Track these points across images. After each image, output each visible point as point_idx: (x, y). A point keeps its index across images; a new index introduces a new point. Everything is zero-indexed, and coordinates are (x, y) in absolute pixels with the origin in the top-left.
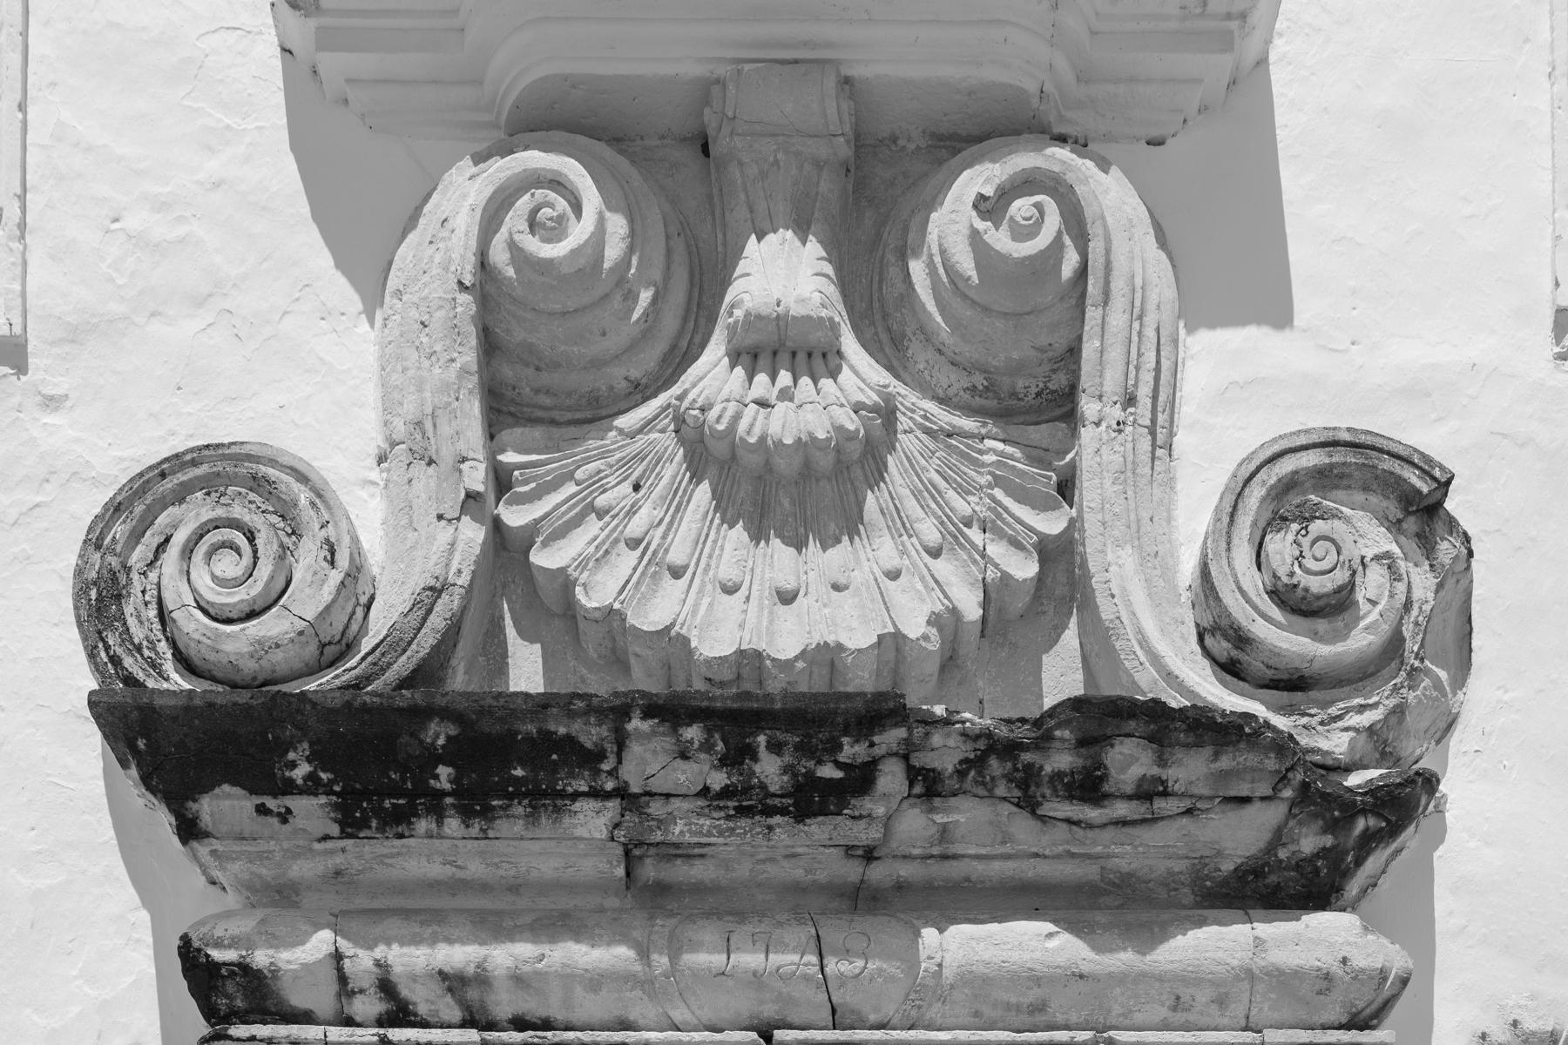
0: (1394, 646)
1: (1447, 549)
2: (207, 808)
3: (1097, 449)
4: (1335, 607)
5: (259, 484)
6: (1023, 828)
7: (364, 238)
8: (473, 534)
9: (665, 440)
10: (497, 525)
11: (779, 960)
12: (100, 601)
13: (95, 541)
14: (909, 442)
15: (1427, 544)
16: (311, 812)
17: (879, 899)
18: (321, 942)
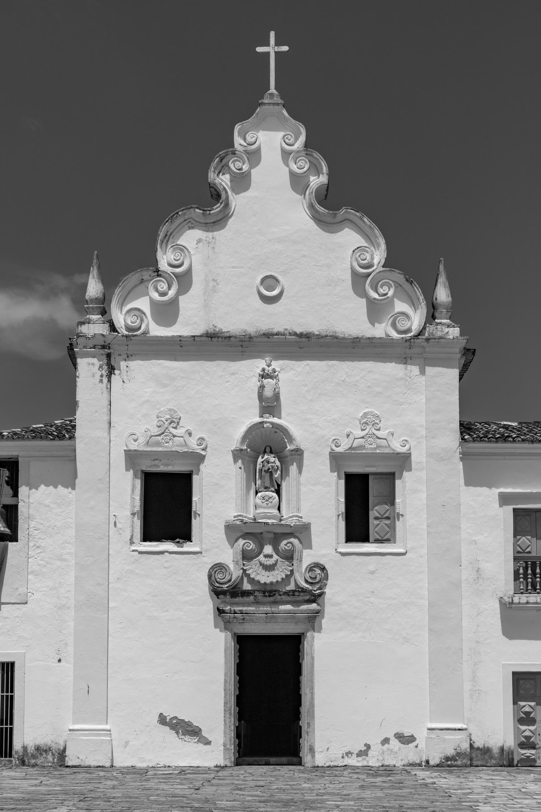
0: (320, 580)
1: (325, 572)
2: (220, 596)
3: (295, 562)
4: (315, 578)
5: (223, 567)
6: (288, 597)
7: (232, 542)
8: (242, 571)
9: (258, 562)
10: (243, 569)
11: (267, 609)
12: (210, 577)
13: (209, 571)
14: (279, 562)
15: (323, 571)
16: (228, 597)
17: (276, 603)
18: (229, 607)
